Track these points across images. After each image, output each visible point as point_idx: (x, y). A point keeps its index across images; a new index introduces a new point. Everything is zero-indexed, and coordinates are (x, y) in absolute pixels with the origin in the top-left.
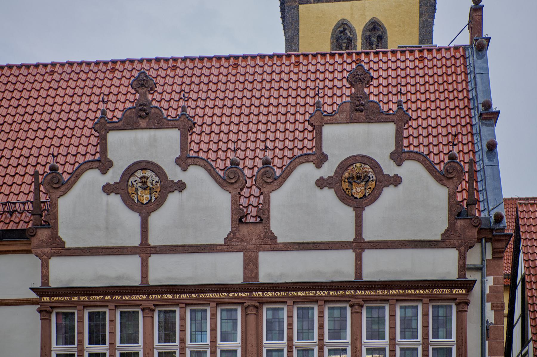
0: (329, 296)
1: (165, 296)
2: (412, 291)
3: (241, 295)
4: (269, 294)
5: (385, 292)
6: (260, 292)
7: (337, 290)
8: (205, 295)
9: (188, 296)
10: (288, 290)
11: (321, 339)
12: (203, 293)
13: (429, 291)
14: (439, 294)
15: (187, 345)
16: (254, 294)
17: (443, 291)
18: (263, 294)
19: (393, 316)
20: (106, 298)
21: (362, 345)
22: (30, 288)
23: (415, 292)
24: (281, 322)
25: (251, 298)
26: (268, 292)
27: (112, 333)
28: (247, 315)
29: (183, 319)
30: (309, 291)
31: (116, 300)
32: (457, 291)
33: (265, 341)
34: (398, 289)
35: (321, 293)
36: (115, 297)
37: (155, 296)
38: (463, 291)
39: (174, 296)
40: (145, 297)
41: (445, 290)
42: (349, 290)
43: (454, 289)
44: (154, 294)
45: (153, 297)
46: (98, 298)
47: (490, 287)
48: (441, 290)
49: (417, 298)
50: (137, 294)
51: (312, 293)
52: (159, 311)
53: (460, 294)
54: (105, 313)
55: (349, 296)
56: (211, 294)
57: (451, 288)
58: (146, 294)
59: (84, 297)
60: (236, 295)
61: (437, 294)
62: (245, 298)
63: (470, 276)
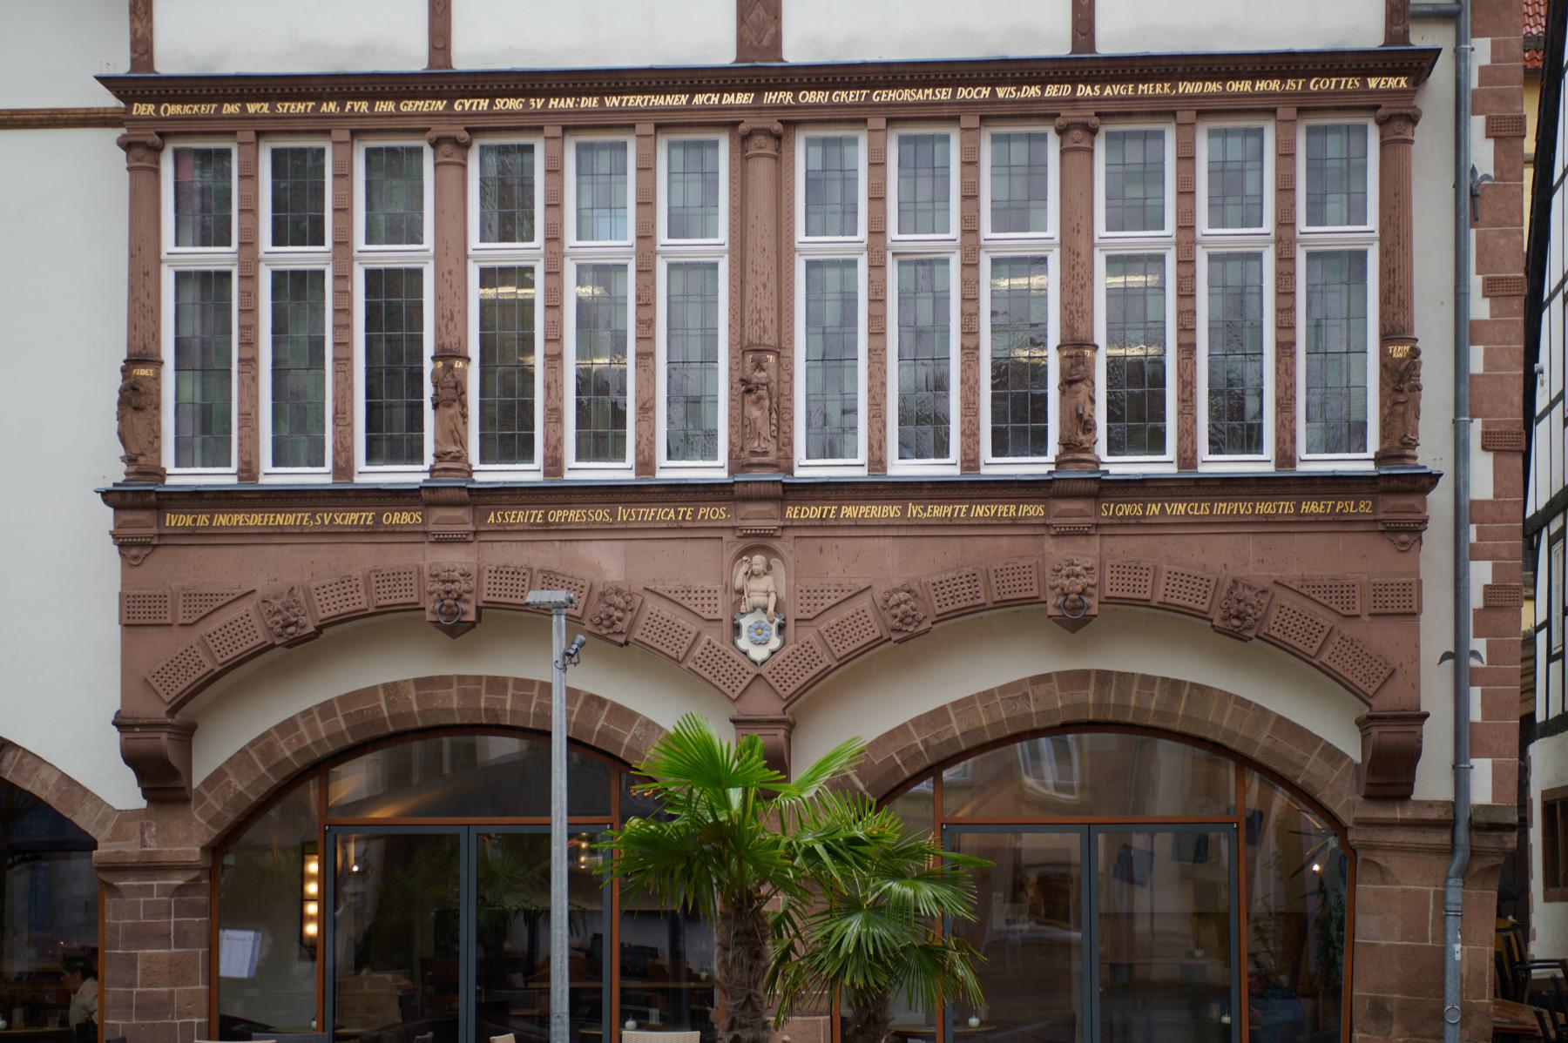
0: (993, 100)
1: (500, 104)
2: (1245, 86)
3: (729, 101)
4: (812, 97)
5: (1162, 89)
6: (786, 90)
7: (1019, 83)
8: (621, 101)
9: (570, 102)
10: (873, 86)
11: (970, 228)
12: (616, 95)
13: (1297, 84)
14: (1328, 93)
15: (566, 249)
16: (770, 98)
17: (1338, 83)
18: (795, 98)
19: (1186, 158)
20: (324, 108)
21: (1093, 245)
22: (98, 78)
23: (1253, 86)
24: (848, 178)
25: (758, 108)
26: (809, 90)
27: (343, 211)
28: (747, 159)
29: (554, 171)
30: (934, 87)
31: (352, 116)
32: (1383, 83)
33: (800, 235)
34: (1204, 80)
35: (969, 93)
36: (352, 106)
37: (472, 105)
38: (1399, 82)
39: (527, 105)
40: (440, 105)
41: (1344, 80)
42: (1053, 84)
43: (1373, 75)
44: (468, 98)
45: (463, 105)
46: (301, 107)
47: (1482, 69)
48: (1334, 80)
49: (1256, 104)
50: (419, 99)
51: (943, 94)
52: (482, 147)
53: (1390, 91)
54: (321, 152)
55: (1052, 100)
56: (639, 99)
57: (1365, 73)
58: (442, 99)
59: (258, 106)
60: (715, 99)
61: (1320, 93)
62: (741, 108)
63: (1421, 38)
